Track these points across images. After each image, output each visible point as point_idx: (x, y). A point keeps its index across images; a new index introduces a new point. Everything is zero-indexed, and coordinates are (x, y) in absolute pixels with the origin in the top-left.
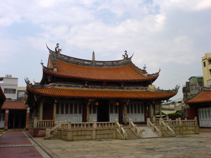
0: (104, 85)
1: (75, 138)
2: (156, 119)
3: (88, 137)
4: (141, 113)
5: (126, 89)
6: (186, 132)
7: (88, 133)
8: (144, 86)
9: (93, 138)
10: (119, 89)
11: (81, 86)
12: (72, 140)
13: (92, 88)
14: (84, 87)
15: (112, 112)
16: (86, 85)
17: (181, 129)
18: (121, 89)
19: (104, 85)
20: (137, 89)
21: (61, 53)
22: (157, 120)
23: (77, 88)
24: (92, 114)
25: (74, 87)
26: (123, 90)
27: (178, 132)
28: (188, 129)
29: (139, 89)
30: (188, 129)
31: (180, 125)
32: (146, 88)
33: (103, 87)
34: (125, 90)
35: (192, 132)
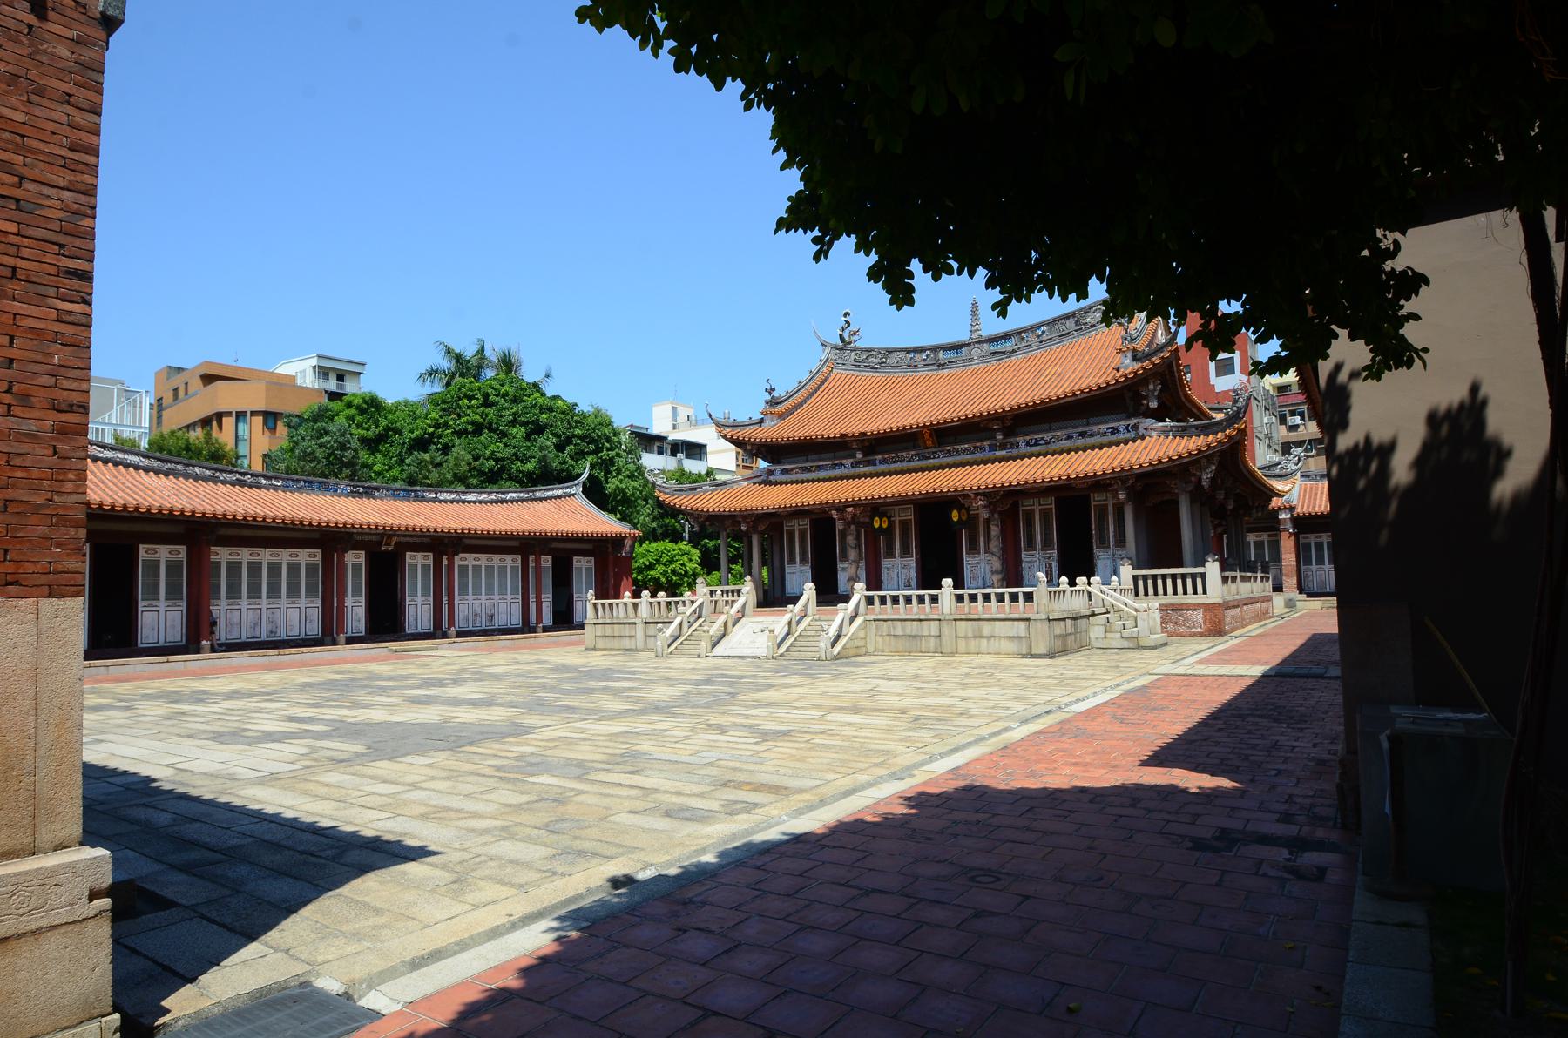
0: (929, 443)
1: (601, 643)
2: (1135, 578)
3: (627, 643)
4: (1116, 546)
5: (1028, 444)
6: (973, 643)
7: (627, 630)
8: (1129, 418)
9: (640, 645)
10: (993, 448)
11: (847, 462)
12: (594, 649)
13: (885, 461)
14: (858, 463)
15: (973, 548)
16: (859, 456)
17: (947, 630)
18: (1003, 447)
19: (929, 443)
20: (1083, 435)
21: (858, 344)
22: (1145, 578)
23: (837, 472)
24: (898, 561)
25: (826, 468)
26: (1015, 452)
27: (932, 643)
28: (986, 632)
29: (1091, 435)
30: (986, 632)
31: (946, 610)
32: (1133, 421)
33: (926, 452)
34: (1023, 449)
35: (1007, 646)
